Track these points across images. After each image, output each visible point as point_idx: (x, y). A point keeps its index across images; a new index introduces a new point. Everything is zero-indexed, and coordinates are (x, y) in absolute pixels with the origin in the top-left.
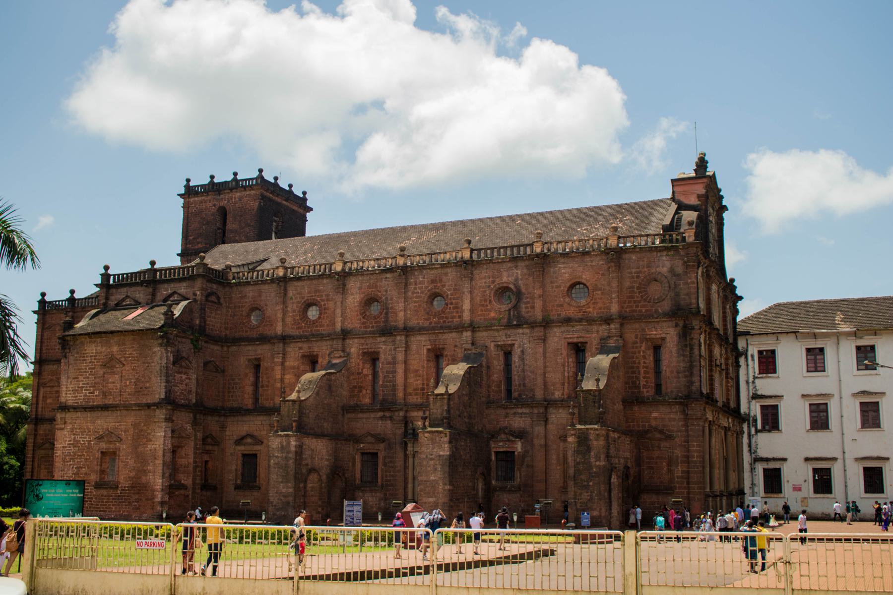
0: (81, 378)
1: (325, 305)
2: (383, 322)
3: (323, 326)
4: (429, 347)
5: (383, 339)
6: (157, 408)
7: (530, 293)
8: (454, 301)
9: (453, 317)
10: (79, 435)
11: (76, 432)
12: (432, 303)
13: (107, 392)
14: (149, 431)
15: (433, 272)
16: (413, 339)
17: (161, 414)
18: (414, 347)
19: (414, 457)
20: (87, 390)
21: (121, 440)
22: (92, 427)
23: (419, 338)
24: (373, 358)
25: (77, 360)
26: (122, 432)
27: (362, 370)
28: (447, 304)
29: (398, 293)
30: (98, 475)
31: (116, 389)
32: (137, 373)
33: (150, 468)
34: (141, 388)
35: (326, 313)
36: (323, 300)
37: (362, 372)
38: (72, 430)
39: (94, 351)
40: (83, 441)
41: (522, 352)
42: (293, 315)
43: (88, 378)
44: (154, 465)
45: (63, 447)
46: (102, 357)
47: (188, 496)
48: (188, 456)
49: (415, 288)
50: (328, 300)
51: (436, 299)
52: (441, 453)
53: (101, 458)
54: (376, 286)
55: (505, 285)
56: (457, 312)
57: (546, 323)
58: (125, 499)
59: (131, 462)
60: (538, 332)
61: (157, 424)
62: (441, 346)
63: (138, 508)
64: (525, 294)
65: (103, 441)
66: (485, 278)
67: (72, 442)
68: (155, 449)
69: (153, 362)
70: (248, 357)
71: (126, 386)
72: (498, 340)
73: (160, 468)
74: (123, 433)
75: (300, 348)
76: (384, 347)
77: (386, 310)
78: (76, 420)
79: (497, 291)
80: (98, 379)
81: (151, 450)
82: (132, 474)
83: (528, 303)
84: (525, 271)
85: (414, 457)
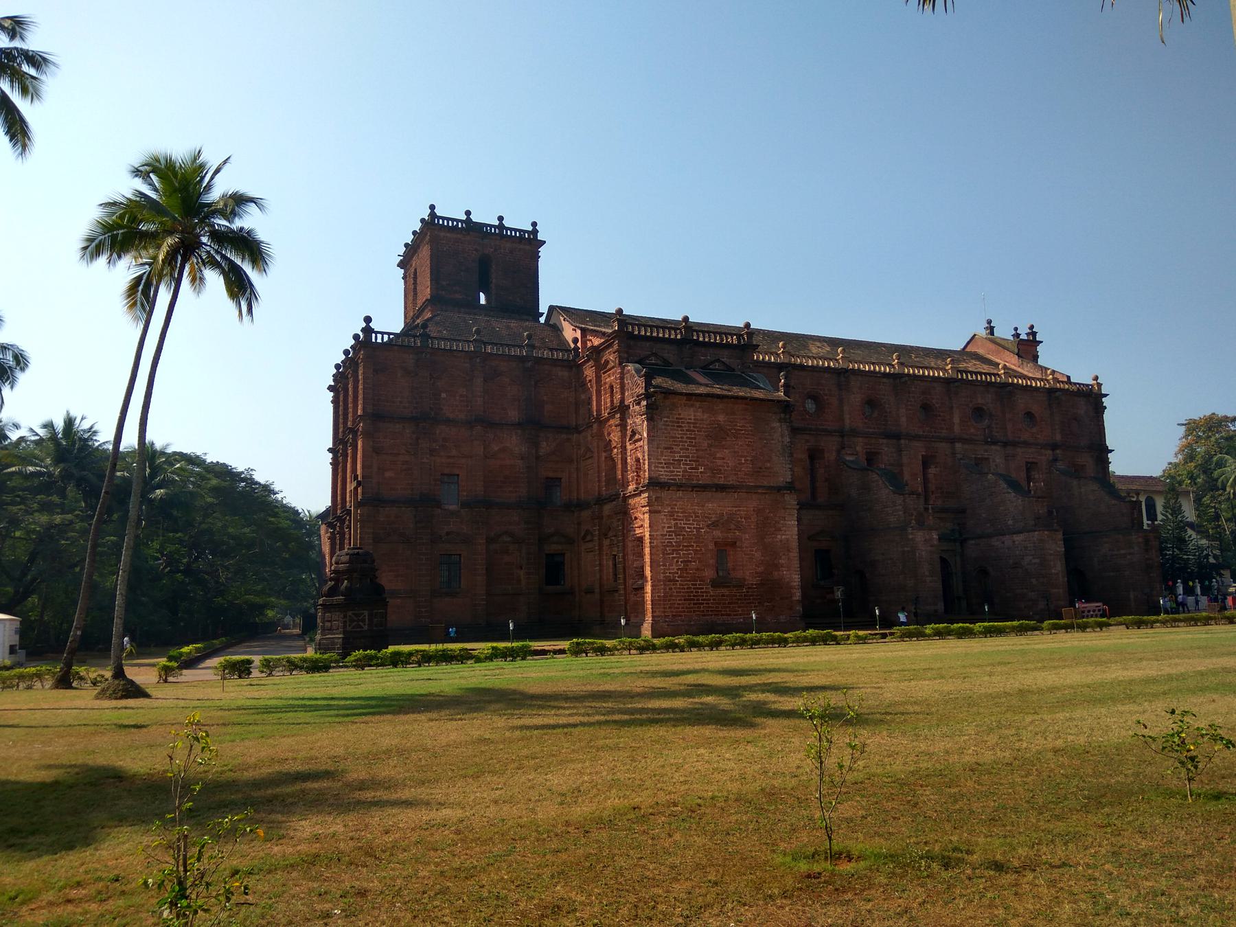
5: (885, 441)
8: (942, 414)
10: (682, 520)
14: (777, 519)
17: (791, 500)
20: (687, 464)
25: (668, 425)
34: (761, 468)
38: (671, 514)
52: (1058, 549)
57: (1014, 444)
58: (754, 599)
59: (758, 555)
61: (788, 511)
76: (886, 449)
78: (677, 501)
81: (781, 541)
82: (760, 569)
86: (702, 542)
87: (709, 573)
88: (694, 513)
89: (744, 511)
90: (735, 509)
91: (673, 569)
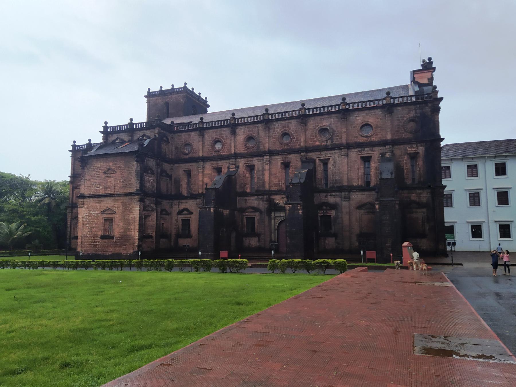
0: (92, 180)
1: (225, 141)
2: (257, 149)
3: (224, 152)
4: (282, 162)
5: (257, 158)
6: (135, 195)
7: (339, 131)
9: (296, 145)
10: (92, 210)
11: (90, 209)
12: (283, 139)
13: (107, 187)
14: (131, 207)
15: (284, 122)
16: (273, 157)
17: (137, 198)
18: (274, 162)
19: (275, 219)
20: (95, 186)
21: (116, 212)
22: (99, 206)
23: (276, 157)
24: (251, 168)
26: (116, 208)
27: (246, 174)
28: (292, 139)
29: (265, 134)
30: (103, 232)
31: (112, 185)
32: (124, 176)
33: (132, 227)
34: (126, 184)
35: (226, 145)
36: (223, 139)
37: (246, 176)
38: (88, 208)
39: (99, 165)
40: (94, 213)
41: (335, 162)
42: (208, 147)
43: (96, 180)
44: (134, 226)
45: (83, 217)
46: (104, 168)
47: (153, 242)
48: (152, 221)
49: (274, 131)
50: (226, 139)
51: (285, 137)
53: (104, 223)
54: (253, 131)
55: (324, 127)
56: (297, 143)
59: (121, 224)
60: (344, 151)
62: (288, 161)
63: (125, 249)
64: (336, 132)
65: (104, 214)
66: (313, 124)
67: (88, 215)
68: (135, 217)
69: (132, 170)
70: (184, 170)
71: (117, 183)
72: (321, 156)
73: (138, 227)
74: (116, 209)
75: (213, 164)
76: (257, 163)
77: (258, 143)
79: (320, 130)
80: (101, 180)
81: (132, 218)
83: (338, 136)
84: (336, 119)
85: (275, 219)
86: (99, 219)
87: (100, 233)
88: (96, 207)
89: (117, 204)
90: (114, 204)
91: (86, 231)
